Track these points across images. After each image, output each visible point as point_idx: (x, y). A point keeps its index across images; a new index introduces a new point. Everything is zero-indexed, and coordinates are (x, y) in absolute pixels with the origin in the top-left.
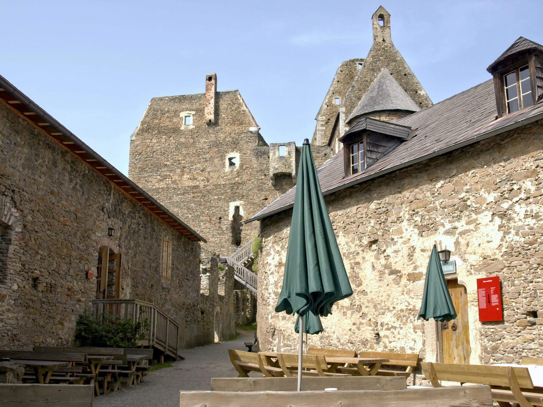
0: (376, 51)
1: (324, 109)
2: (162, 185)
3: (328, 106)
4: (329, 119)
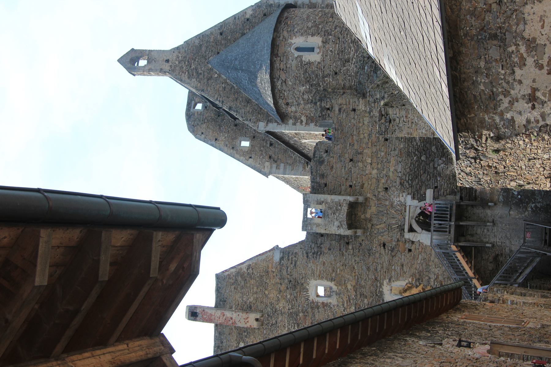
0: (183, 72)
1: (253, 164)
3: (251, 158)
4: (270, 157)
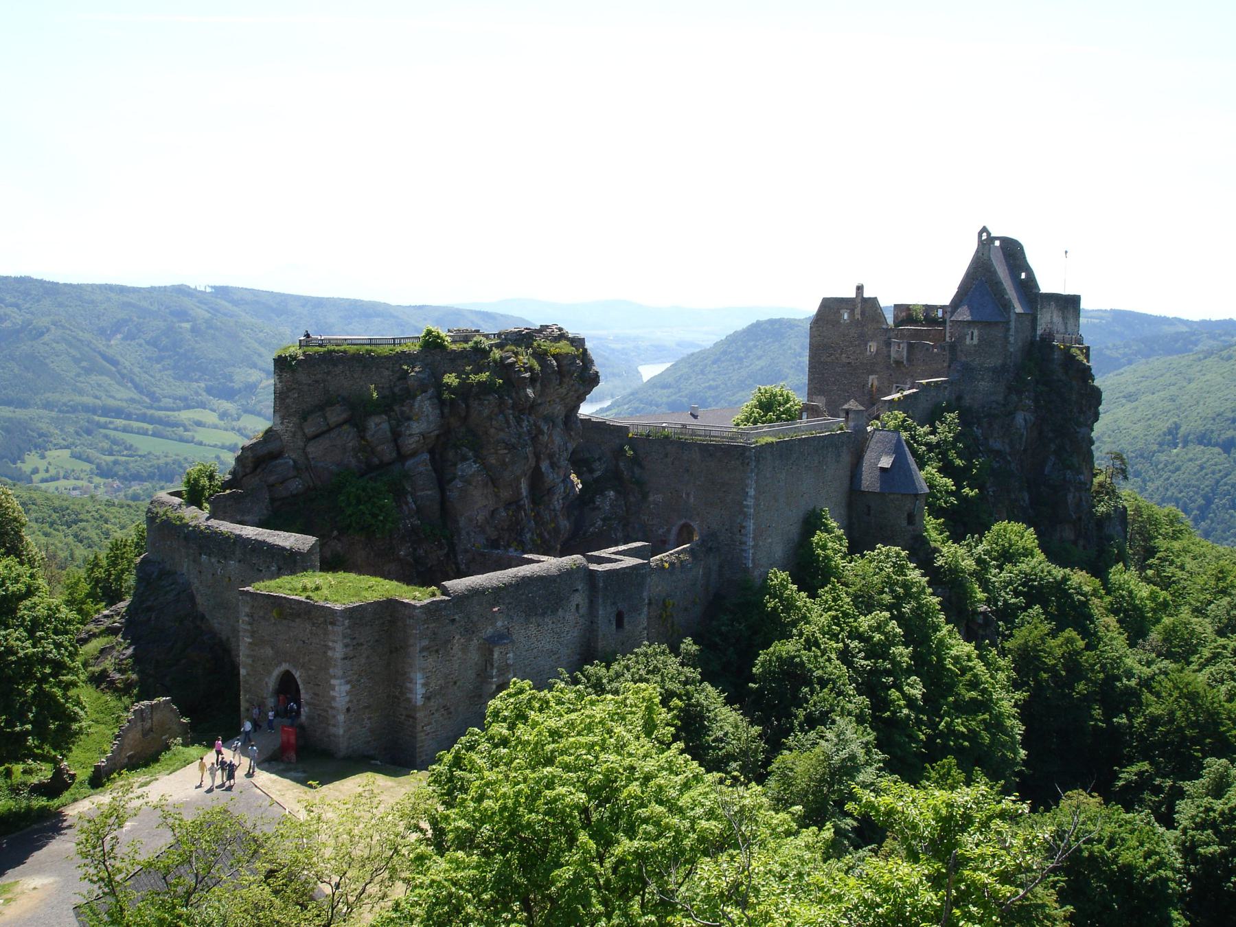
2: (829, 360)
